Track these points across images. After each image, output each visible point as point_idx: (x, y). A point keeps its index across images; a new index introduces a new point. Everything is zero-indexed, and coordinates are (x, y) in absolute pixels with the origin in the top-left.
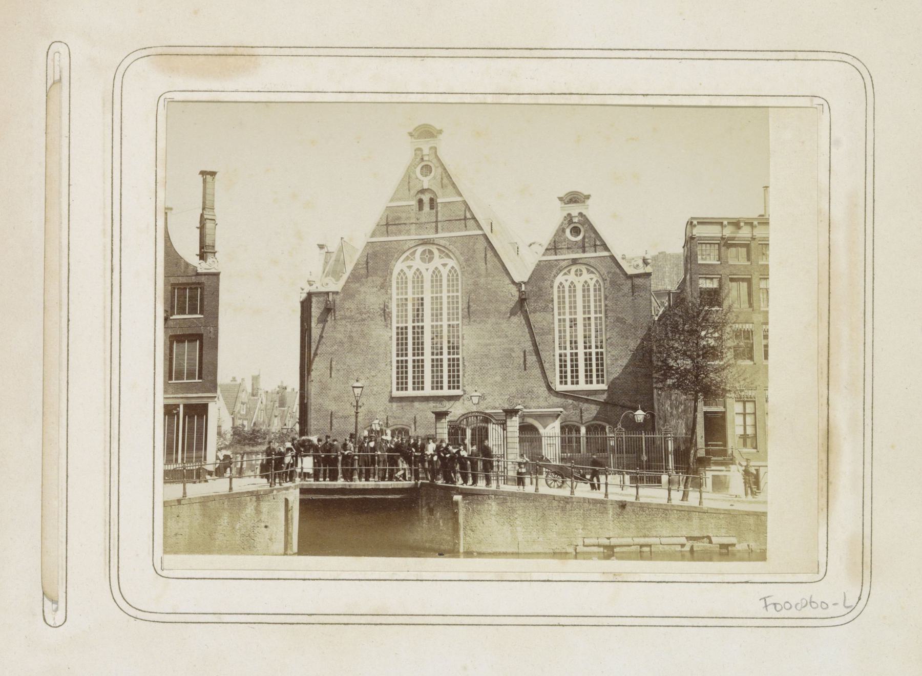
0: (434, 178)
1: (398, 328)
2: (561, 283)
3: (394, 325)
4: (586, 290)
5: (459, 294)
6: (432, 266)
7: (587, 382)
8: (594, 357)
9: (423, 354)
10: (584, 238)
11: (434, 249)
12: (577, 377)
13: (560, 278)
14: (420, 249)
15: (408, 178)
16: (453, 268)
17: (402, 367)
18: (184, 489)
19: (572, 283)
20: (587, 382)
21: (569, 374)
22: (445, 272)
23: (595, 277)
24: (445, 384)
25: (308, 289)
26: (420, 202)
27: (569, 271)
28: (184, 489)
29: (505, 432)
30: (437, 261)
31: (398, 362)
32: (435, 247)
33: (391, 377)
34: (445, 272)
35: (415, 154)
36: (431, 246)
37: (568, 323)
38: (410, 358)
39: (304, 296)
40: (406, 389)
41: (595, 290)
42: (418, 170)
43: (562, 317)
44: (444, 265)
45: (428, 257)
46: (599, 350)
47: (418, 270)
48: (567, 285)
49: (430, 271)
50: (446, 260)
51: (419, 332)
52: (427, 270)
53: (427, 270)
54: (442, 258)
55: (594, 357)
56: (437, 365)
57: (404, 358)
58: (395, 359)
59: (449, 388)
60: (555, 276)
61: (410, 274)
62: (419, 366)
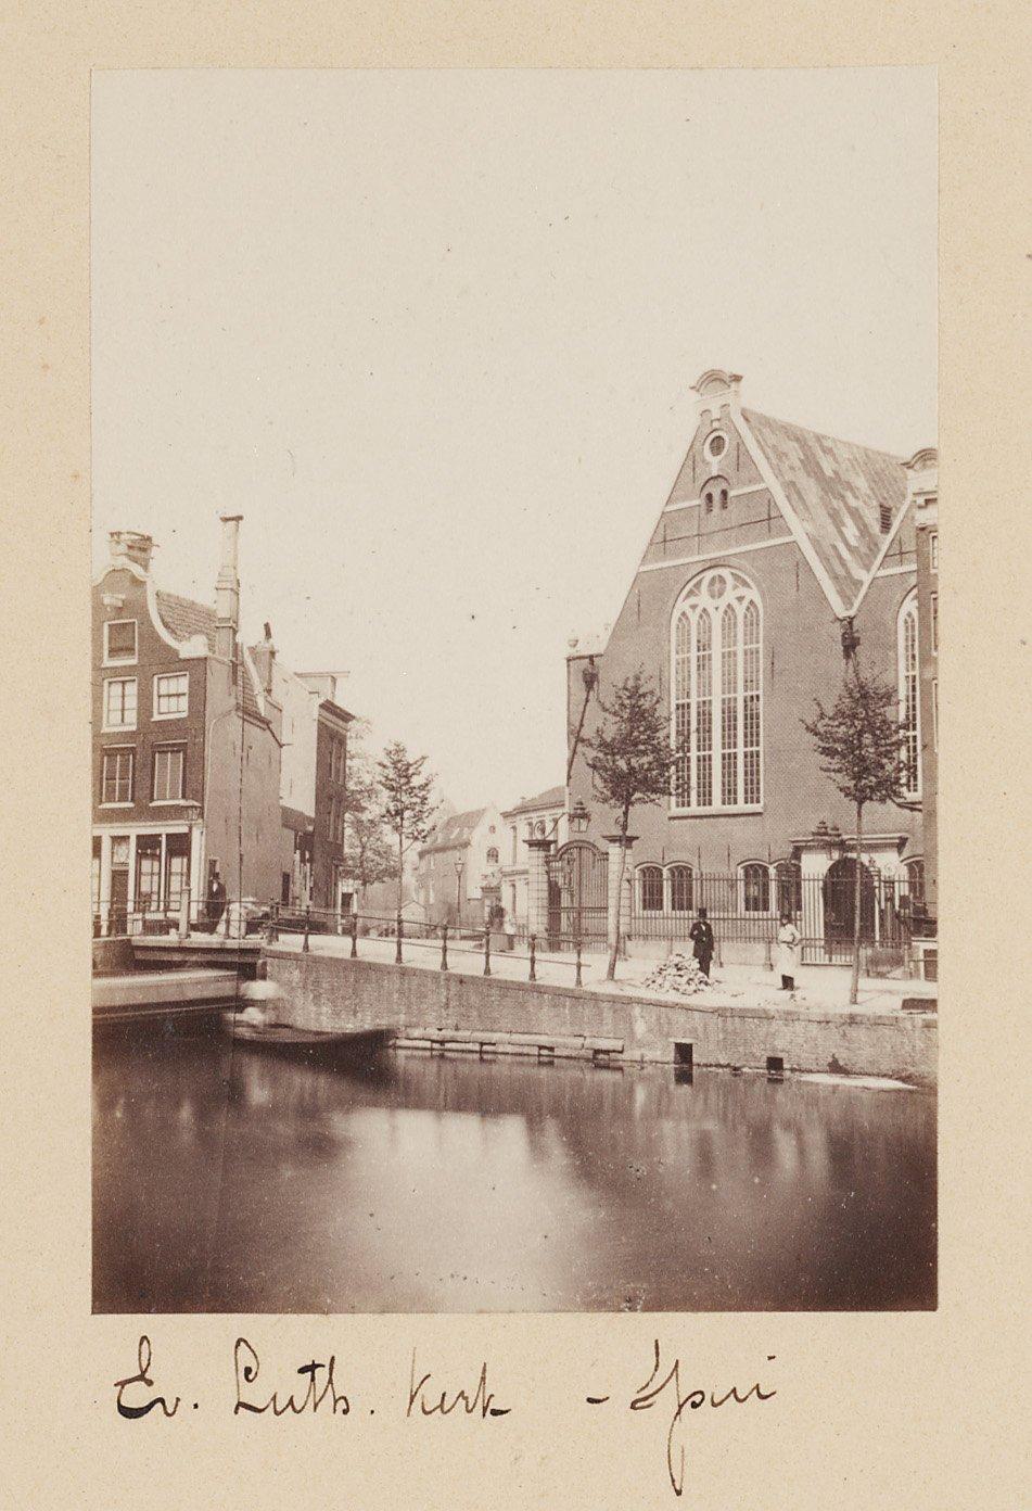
6: (722, 603)
11: (725, 572)
15: (692, 460)
18: (306, 940)
26: (709, 497)
28: (306, 940)
30: (730, 596)
36: (723, 569)
44: (740, 599)
49: (721, 610)
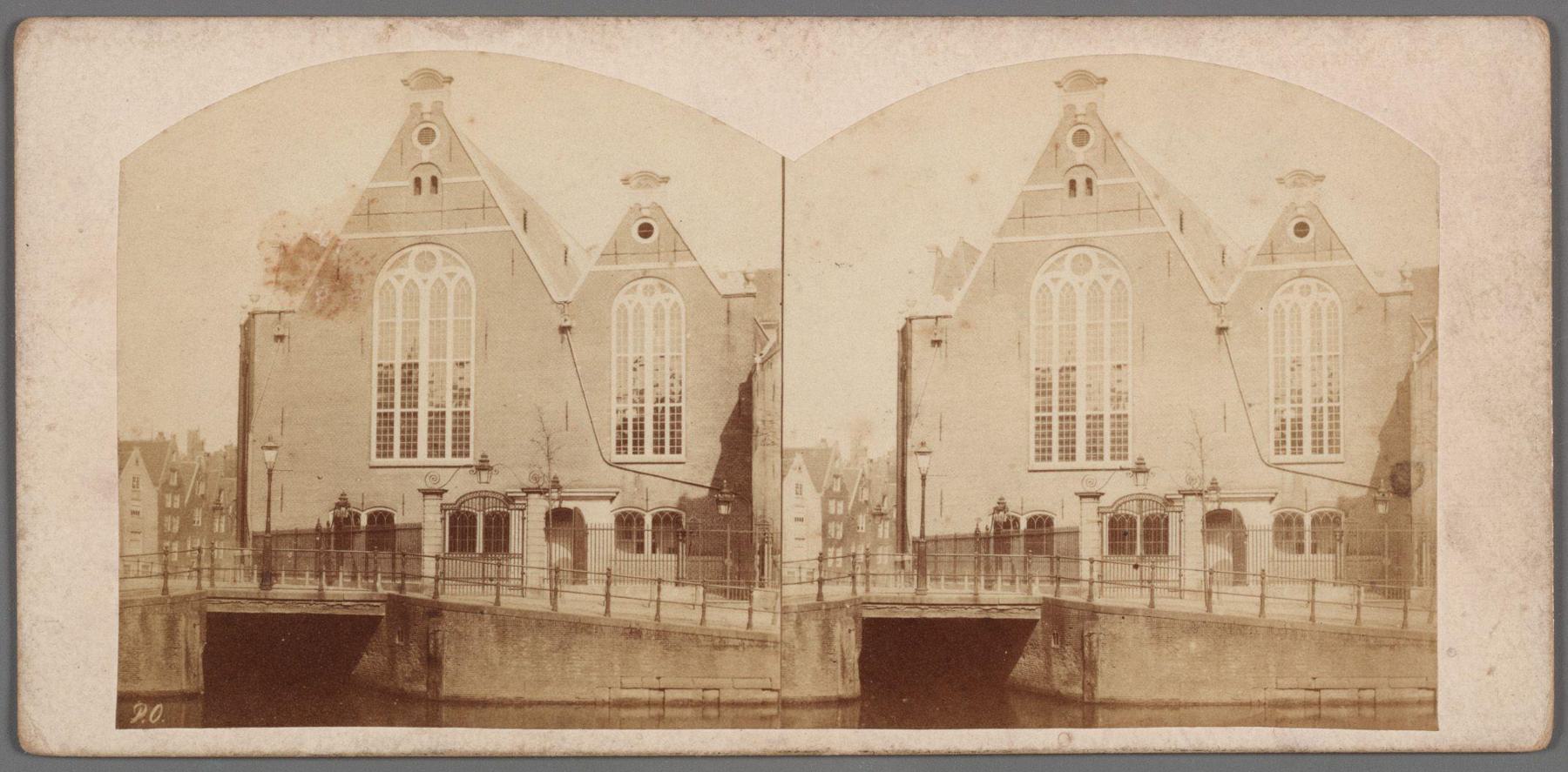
0: (439, 145)
1: (380, 365)
2: (622, 306)
3: (375, 362)
4: (659, 315)
5: (473, 318)
6: (432, 276)
7: (655, 451)
8: (667, 414)
9: (416, 406)
10: (659, 239)
12: (642, 443)
13: (621, 299)
14: (417, 250)
16: (463, 279)
17: (386, 420)
19: (639, 305)
20: (655, 451)
21: (630, 439)
22: (451, 285)
23: (675, 296)
24: (448, 450)
25: (251, 308)
27: (635, 288)
29: (525, 521)
30: (438, 272)
31: (379, 415)
32: (438, 248)
33: (370, 437)
34: (451, 285)
35: (411, 111)
37: (631, 365)
38: (397, 410)
39: (245, 317)
40: (391, 455)
41: (672, 317)
42: (416, 132)
43: (623, 355)
45: (426, 263)
46: (676, 405)
47: (411, 281)
48: (630, 308)
50: (451, 269)
51: (410, 370)
52: (425, 281)
53: (425, 281)
54: (448, 265)
55: (667, 414)
56: (437, 419)
57: (389, 410)
58: (375, 410)
59: (454, 455)
60: (614, 295)
61: (400, 287)
62: (410, 419)
